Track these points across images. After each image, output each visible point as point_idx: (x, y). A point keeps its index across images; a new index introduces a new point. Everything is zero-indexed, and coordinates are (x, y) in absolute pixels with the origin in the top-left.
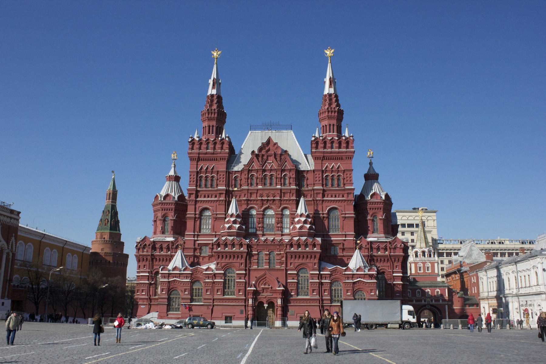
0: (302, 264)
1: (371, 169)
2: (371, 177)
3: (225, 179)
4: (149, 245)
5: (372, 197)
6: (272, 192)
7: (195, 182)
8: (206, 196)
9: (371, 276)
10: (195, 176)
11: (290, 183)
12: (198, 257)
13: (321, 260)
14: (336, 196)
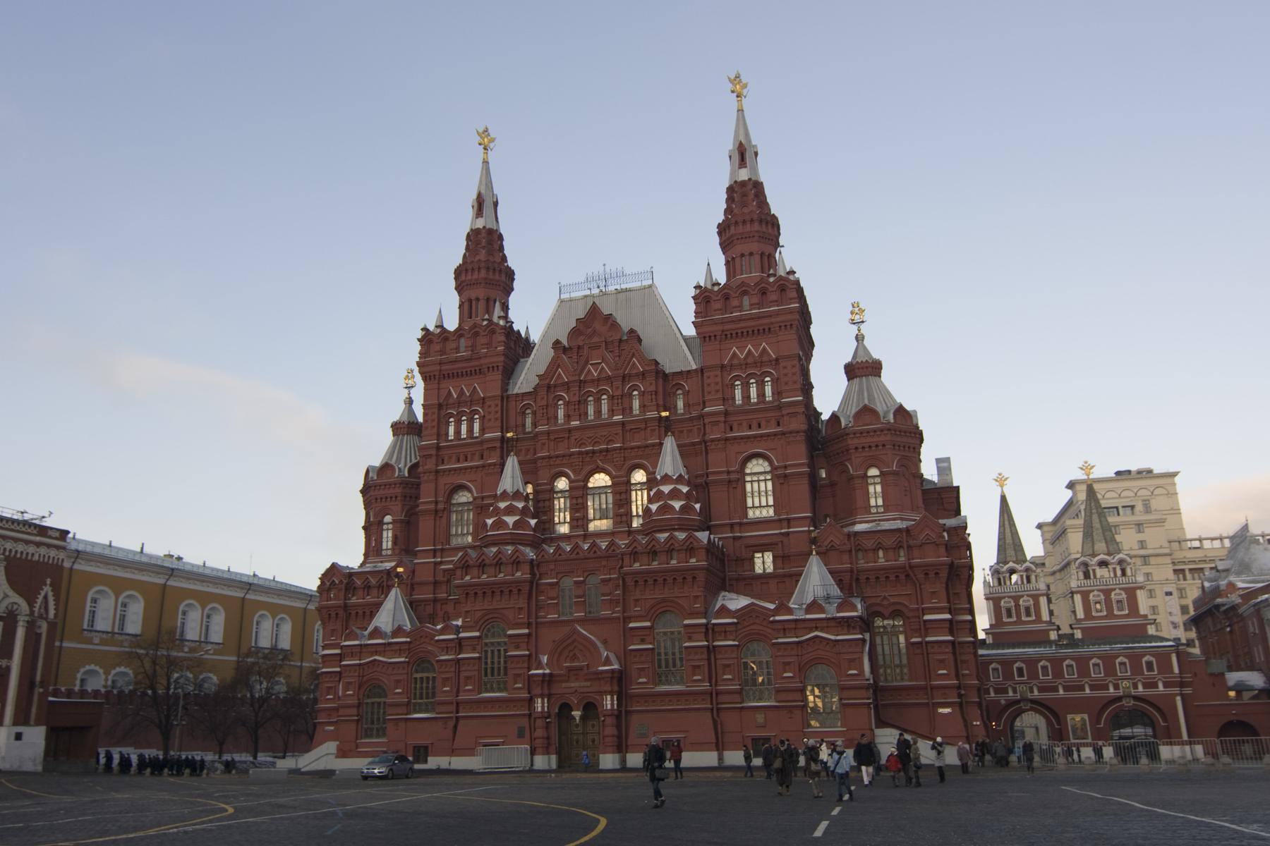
0: (664, 600)
1: (861, 352)
2: (863, 369)
3: (499, 415)
4: (341, 582)
7: (435, 430)
8: (462, 457)
9: (847, 624)
12: (445, 601)
14: (759, 426)
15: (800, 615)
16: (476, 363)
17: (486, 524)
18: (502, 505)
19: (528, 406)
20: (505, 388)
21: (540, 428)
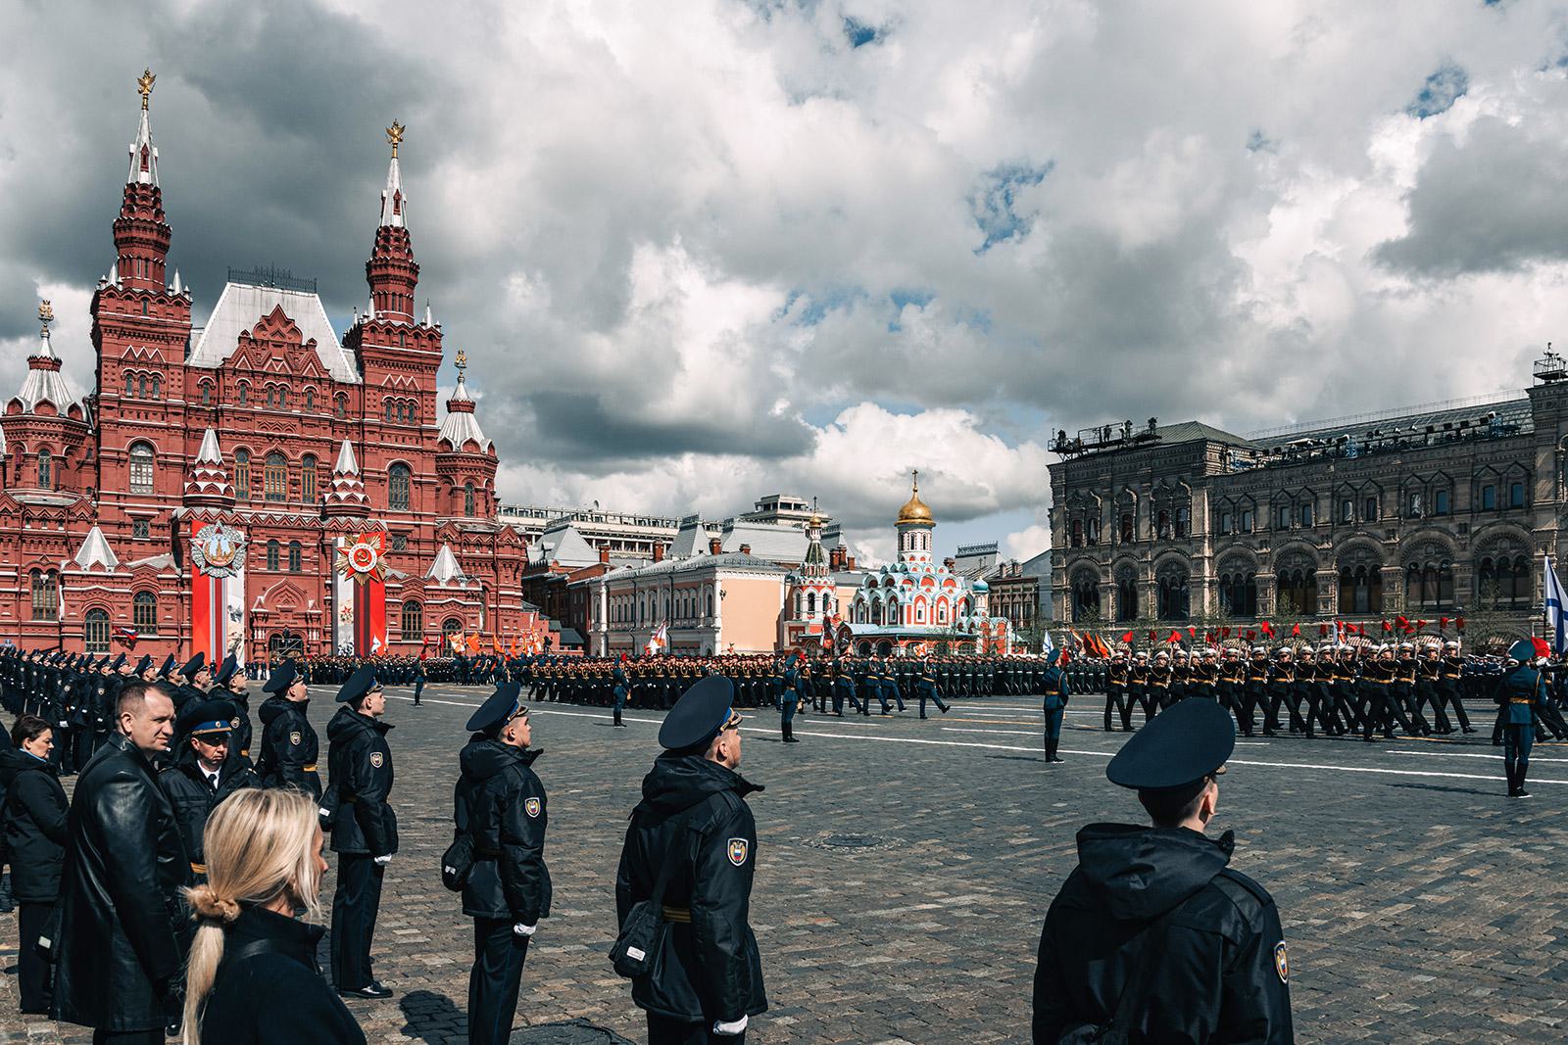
6: (283, 421)
8: (143, 415)
15: (443, 586)
16: (162, 330)
17: (198, 487)
18: (212, 472)
19: (206, 382)
21: (225, 406)
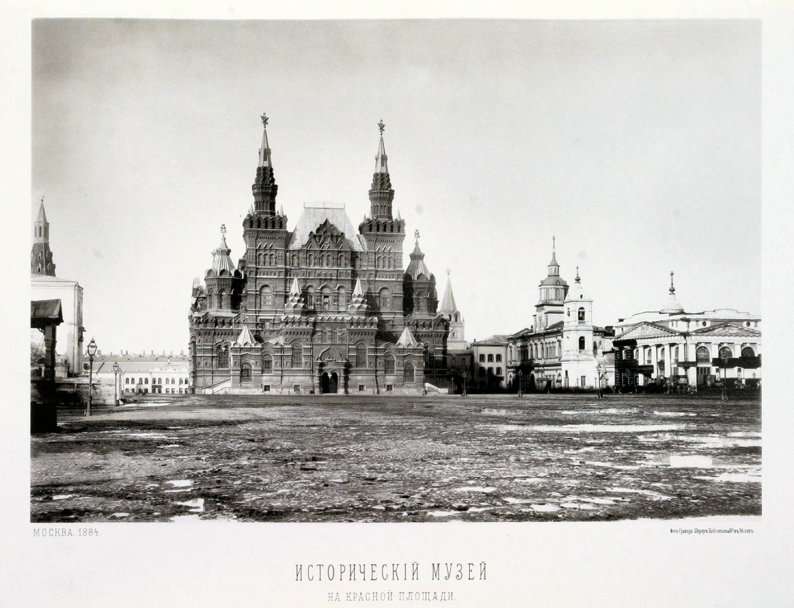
2: (417, 257)
5: (418, 277)
7: (254, 260)
10: (254, 254)
11: (346, 264)
13: (376, 337)
20: (287, 246)
